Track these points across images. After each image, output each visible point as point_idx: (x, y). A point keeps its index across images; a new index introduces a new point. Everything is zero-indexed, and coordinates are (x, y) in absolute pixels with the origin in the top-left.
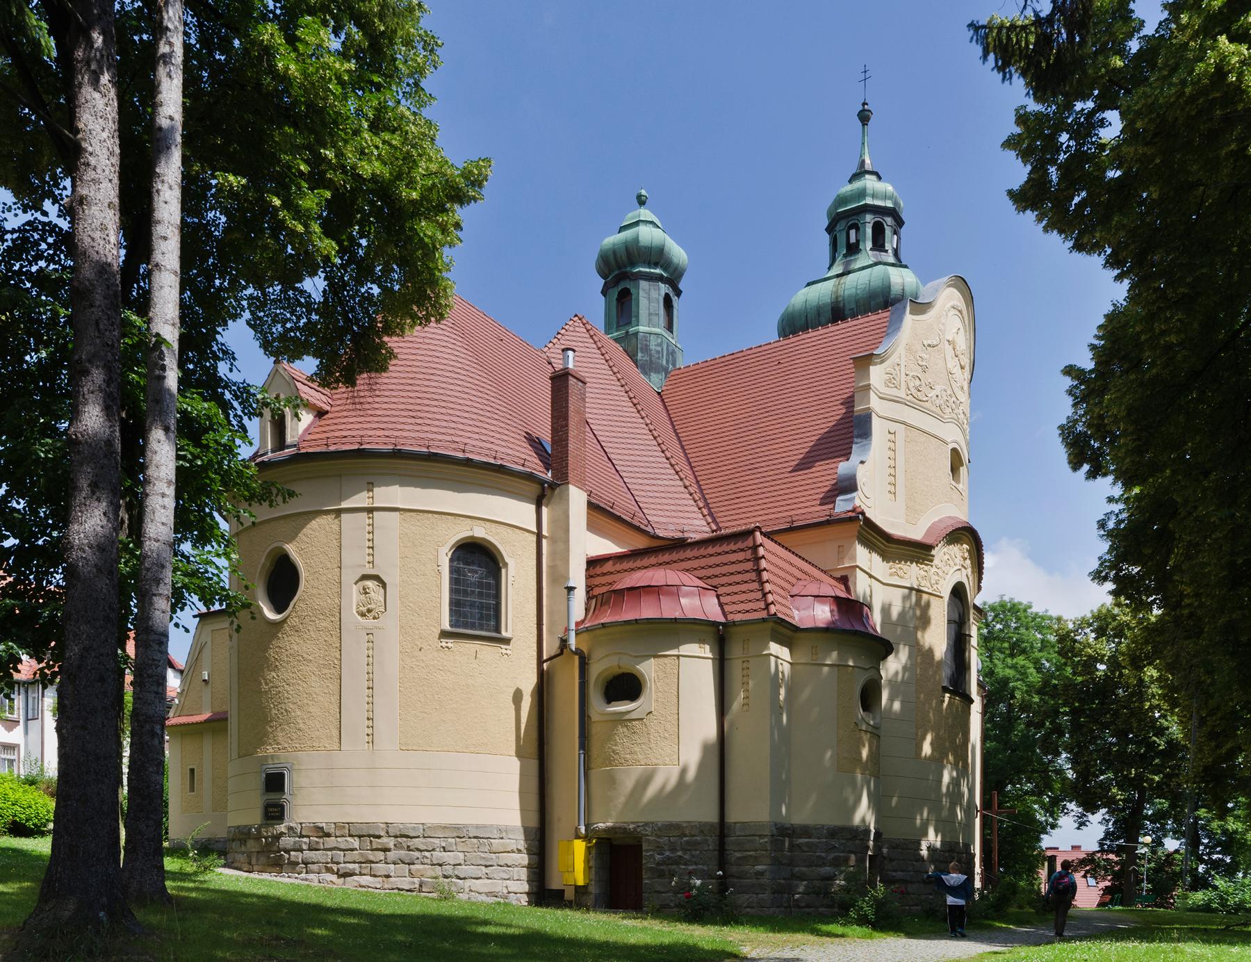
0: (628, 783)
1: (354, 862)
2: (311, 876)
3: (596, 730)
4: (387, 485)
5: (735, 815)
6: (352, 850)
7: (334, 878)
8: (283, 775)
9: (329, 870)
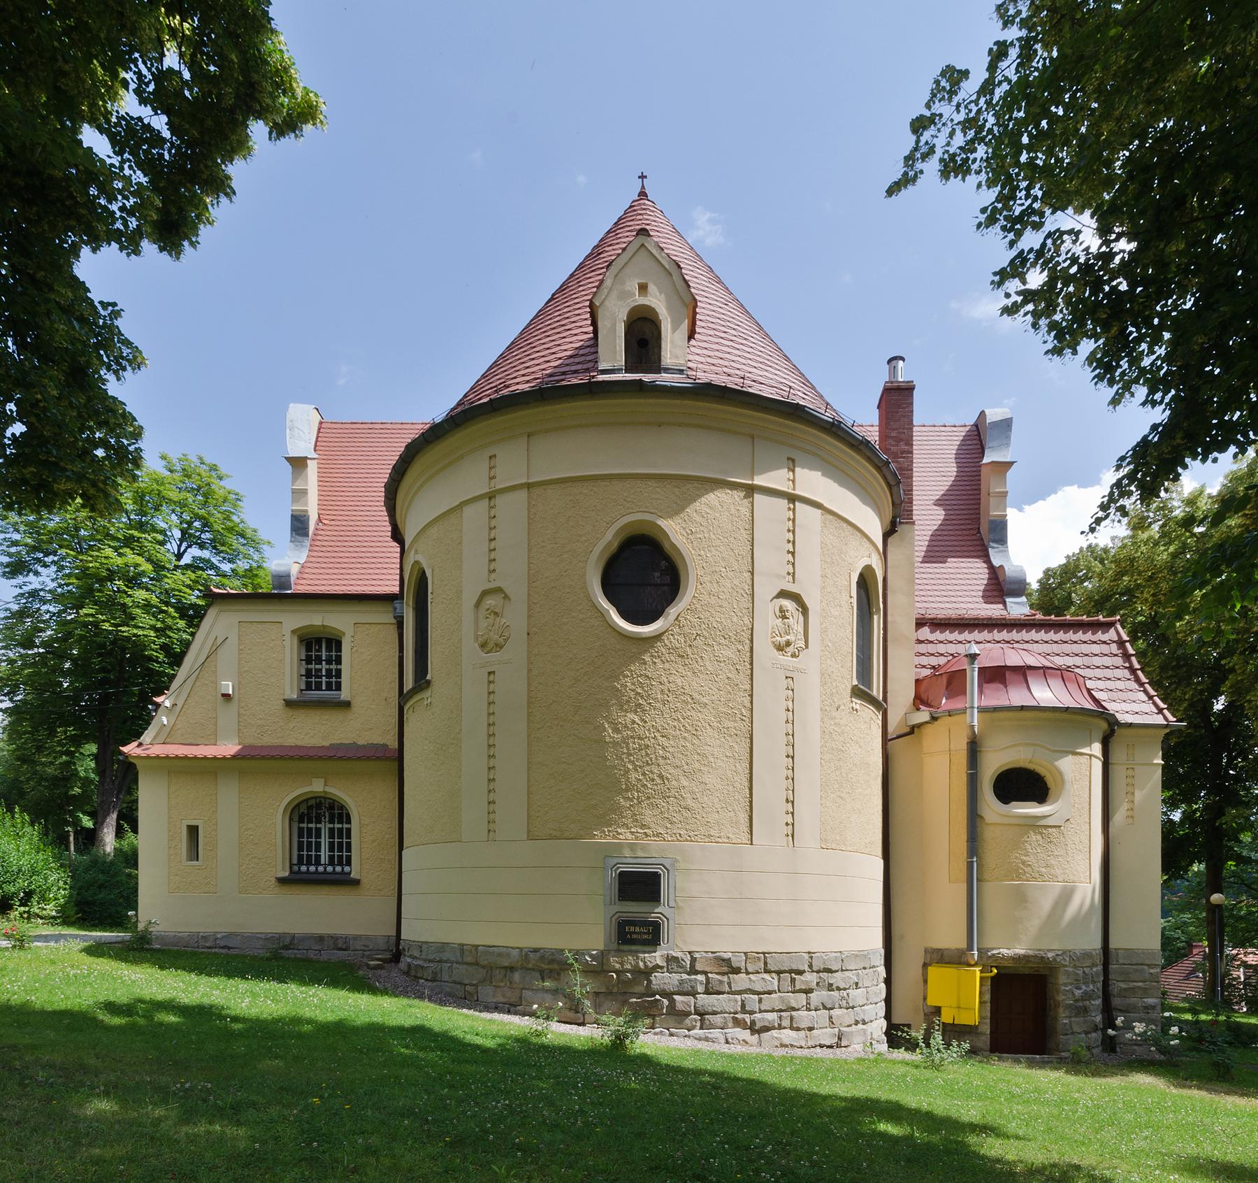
0: (1046, 904)
1: (773, 1011)
2: (716, 1033)
3: (992, 836)
4: (811, 469)
5: (1113, 944)
6: (769, 993)
7: (746, 1035)
8: (655, 878)
9: (738, 1023)
